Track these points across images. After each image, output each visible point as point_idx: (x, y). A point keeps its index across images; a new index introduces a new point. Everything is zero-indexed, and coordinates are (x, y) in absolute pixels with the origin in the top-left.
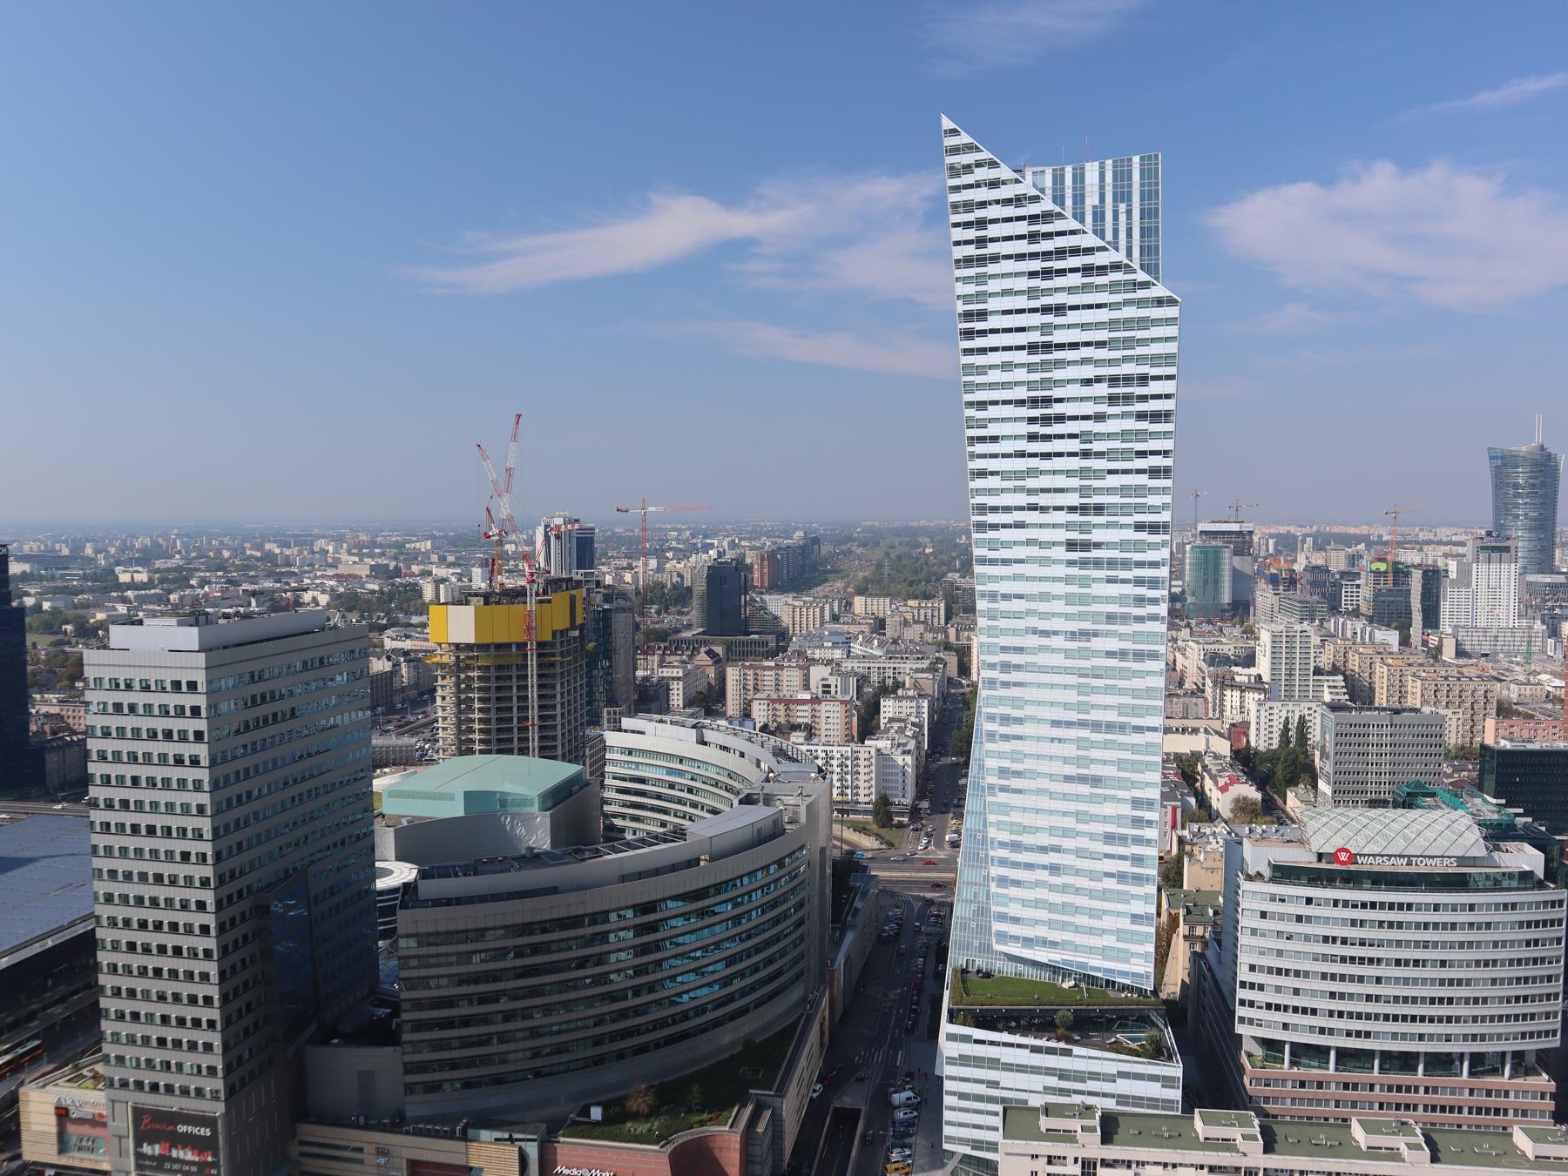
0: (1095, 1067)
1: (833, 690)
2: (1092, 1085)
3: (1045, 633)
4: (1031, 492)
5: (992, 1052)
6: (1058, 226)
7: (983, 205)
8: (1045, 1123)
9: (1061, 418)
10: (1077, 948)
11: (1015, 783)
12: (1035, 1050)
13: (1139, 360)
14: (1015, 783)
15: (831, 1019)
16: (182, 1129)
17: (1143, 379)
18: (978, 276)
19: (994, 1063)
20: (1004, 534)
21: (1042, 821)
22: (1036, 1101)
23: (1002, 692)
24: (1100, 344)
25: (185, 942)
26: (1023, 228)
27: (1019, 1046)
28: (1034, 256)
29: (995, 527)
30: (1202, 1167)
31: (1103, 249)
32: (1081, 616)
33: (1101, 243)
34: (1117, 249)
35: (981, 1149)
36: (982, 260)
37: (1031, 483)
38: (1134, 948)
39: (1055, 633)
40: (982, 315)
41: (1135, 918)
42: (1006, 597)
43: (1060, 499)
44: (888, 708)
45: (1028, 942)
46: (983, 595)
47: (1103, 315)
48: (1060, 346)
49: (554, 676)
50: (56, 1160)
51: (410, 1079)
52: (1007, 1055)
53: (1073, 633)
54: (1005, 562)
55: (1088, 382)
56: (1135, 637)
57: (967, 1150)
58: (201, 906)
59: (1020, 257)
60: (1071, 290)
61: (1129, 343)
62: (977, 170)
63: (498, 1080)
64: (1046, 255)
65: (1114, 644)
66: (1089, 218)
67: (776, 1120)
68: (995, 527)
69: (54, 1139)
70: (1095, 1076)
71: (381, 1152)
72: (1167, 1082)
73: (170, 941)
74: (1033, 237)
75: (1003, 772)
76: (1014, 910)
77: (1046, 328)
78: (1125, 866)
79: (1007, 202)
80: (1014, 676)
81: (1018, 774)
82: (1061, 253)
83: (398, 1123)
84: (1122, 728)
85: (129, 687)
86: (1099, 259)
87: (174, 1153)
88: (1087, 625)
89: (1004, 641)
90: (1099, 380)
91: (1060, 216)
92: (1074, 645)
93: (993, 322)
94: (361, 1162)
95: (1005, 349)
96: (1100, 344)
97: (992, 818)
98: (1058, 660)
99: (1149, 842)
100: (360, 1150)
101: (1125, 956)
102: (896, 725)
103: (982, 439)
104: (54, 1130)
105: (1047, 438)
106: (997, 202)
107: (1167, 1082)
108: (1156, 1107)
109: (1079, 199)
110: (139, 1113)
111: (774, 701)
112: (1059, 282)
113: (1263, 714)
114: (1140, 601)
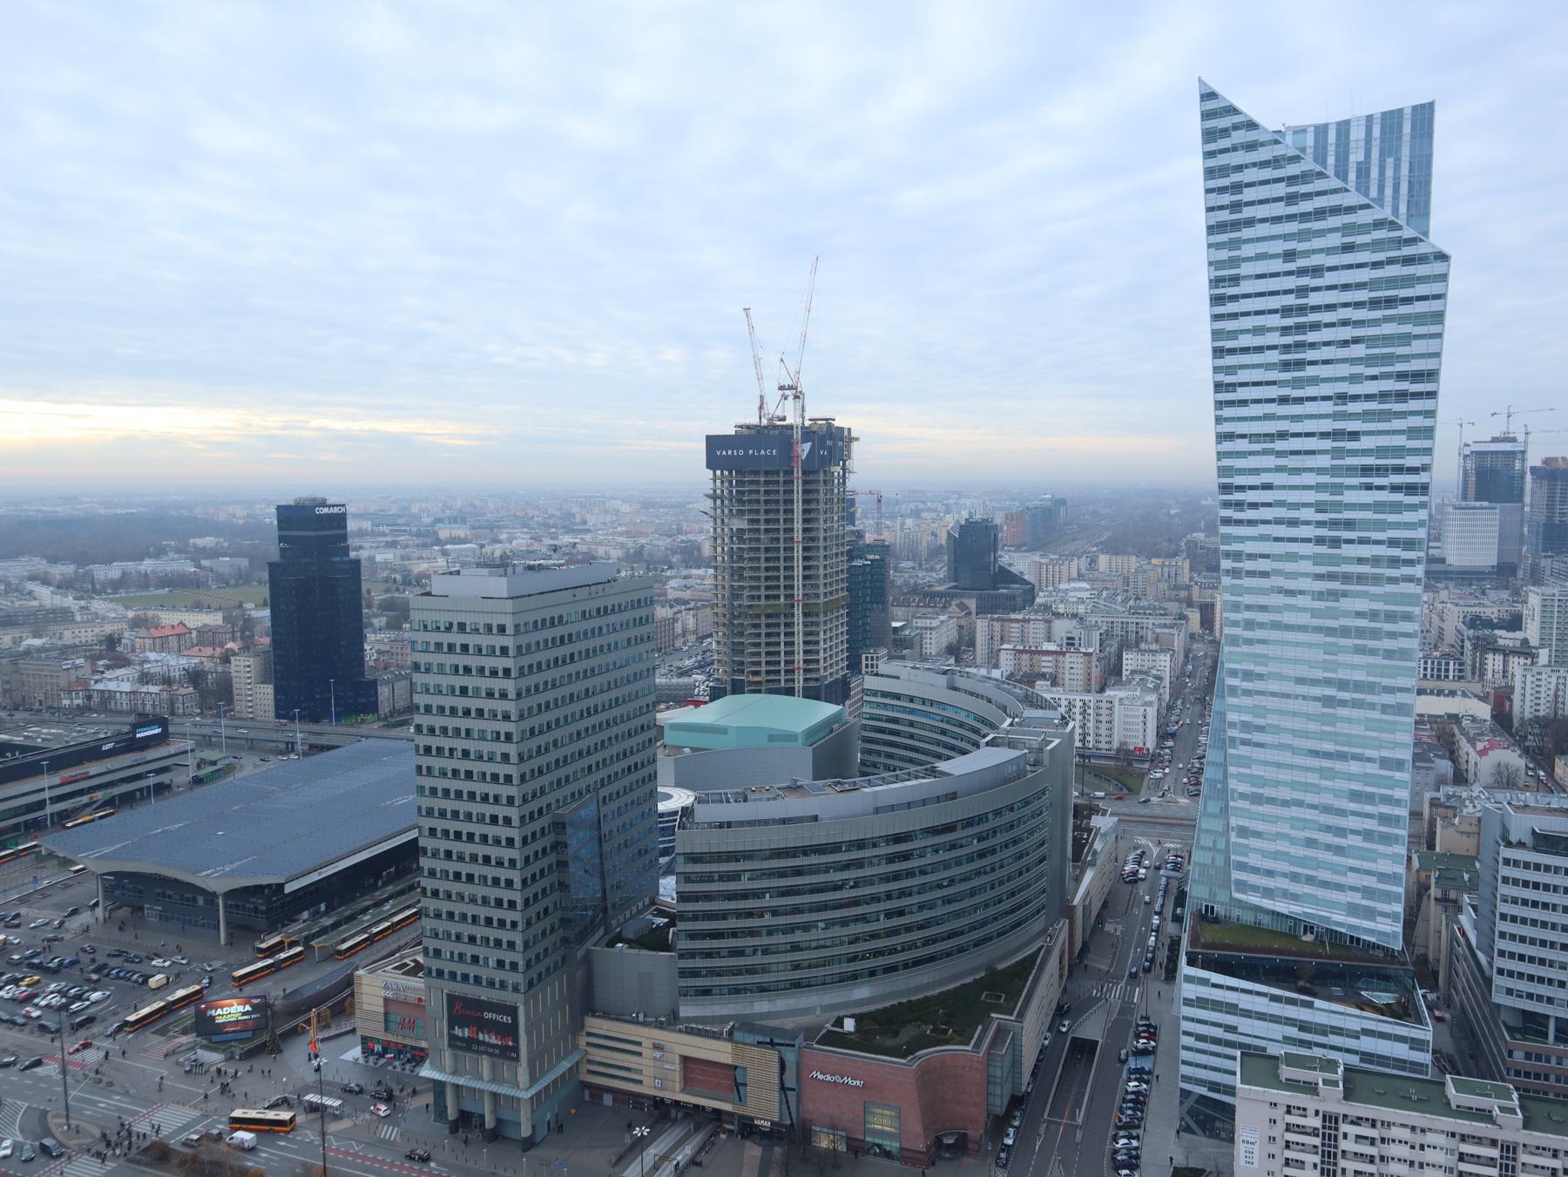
0: (1336, 1021)
1: (1077, 642)
2: (1334, 1040)
3: (1291, 593)
4: (1280, 454)
5: (1231, 997)
6: (1319, 185)
8: (1287, 1072)
9: (1315, 381)
10: (1317, 901)
11: (1257, 737)
12: (1274, 998)
13: (1403, 319)
14: (1257, 737)
15: (1071, 953)
16: (488, 1015)
17: (1406, 339)
18: (1231, 241)
19: (1232, 1009)
20: (1251, 496)
21: (1284, 775)
22: (1274, 1049)
23: (1245, 649)
24: (1358, 305)
25: (494, 852)
26: (1281, 190)
27: (1258, 994)
28: (1291, 218)
29: (1241, 488)
30: (1453, 1135)
31: (1367, 206)
32: (1331, 577)
33: (1363, 200)
34: (1382, 206)
35: (1218, 1091)
36: (1235, 225)
37: (1280, 445)
38: (1380, 906)
39: (1301, 592)
40: (1235, 280)
41: (1383, 877)
42: (1251, 557)
43: (1310, 462)
44: (1130, 661)
45: (1268, 893)
46: (1228, 555)
48: (1316, 309)
49: (817, 624)
50: (382, 1036)
51: (684, 982)
52: (1245, 1002)
53: (1321, 593)
54: (1251, 523)
56: (1387, 598)
57: (1203, 1091)
58: (508, 821)
59: (1277, 220)
60: (1329, 251)
61: (1390, 302)
62: (1234, 134)
63: (763, 989)
64: (1304, 217)
65: (1363, 605)
66: (1352, 176)
67: (1016, 1045)
68: (1241, 488)
69: (382, 1018)
70: (1338, 1031)
71: (657, 1047)
72: (1416, 1044)
73: (481, 850)
74: (1291, 199)
75: (1246, 726)
76: (1254, 860)
77: (1302, 291)
78: (1371, 825)
79: (1263, 164)
80: (1260, 634)
81: (1261, 729)
82: (1320, 214)
83: (672, 1020)
84: (1371, 688)
85: (449, 629)
86: (1364, 217)
87: (481, 1037)
89: (1247, 599)
90: (1356, 341)
91: (1321, 175)
93: (1246, 287)
94: (640, 1054)
95: (1258, 313)
96: (1358, 305)
97: (1232, 769)
98: (1304, 619)
99: (1398, 802)
100: (640, 1044)
101: (1370, 914)
102: (1138, 678)
103: (1231, 403)
104: (382, 1010)
105: (1299, 400)
106: (1254, 165)
107: (1416, 1044)
108: (1404, 1069)
109: (1343, 157)
110: (452, 999)
111: (1019, 651)
112: (1317, 243)
113: (1529, 679)
114: (1395, 562)
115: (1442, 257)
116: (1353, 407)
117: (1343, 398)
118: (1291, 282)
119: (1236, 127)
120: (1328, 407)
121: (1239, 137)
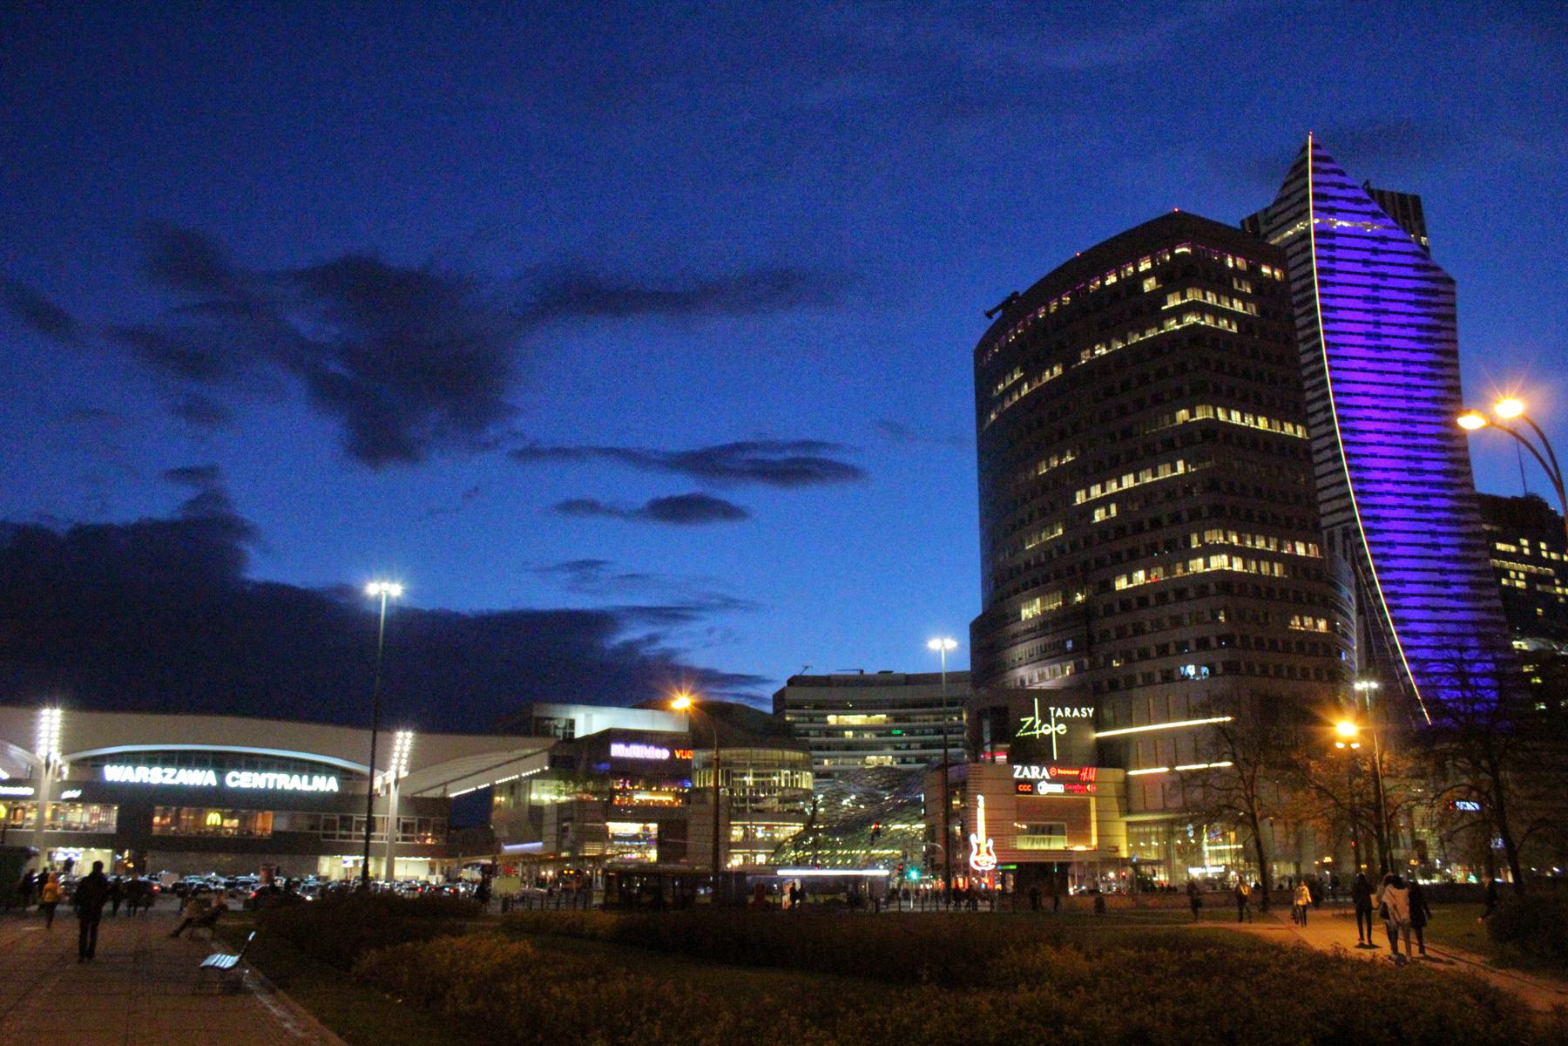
7: (1333, 198)
9: (1388, 348)
40: (1332, 272)
47: (1409, 284)
55: (1403, 326)
61: (1429, 304)
77: (1375, 288)
79: (1348, 200)
88: (1426, 490)
92: (1422, 503)
93: (1340, 278)
112: (1383, 258)
115: (1451, 282)
116: (1413, 369)
117: (1405, 362)
118: (1369, 281)
119: (1334, 171)
120: (1400, 367)
121: (1336, 178)
